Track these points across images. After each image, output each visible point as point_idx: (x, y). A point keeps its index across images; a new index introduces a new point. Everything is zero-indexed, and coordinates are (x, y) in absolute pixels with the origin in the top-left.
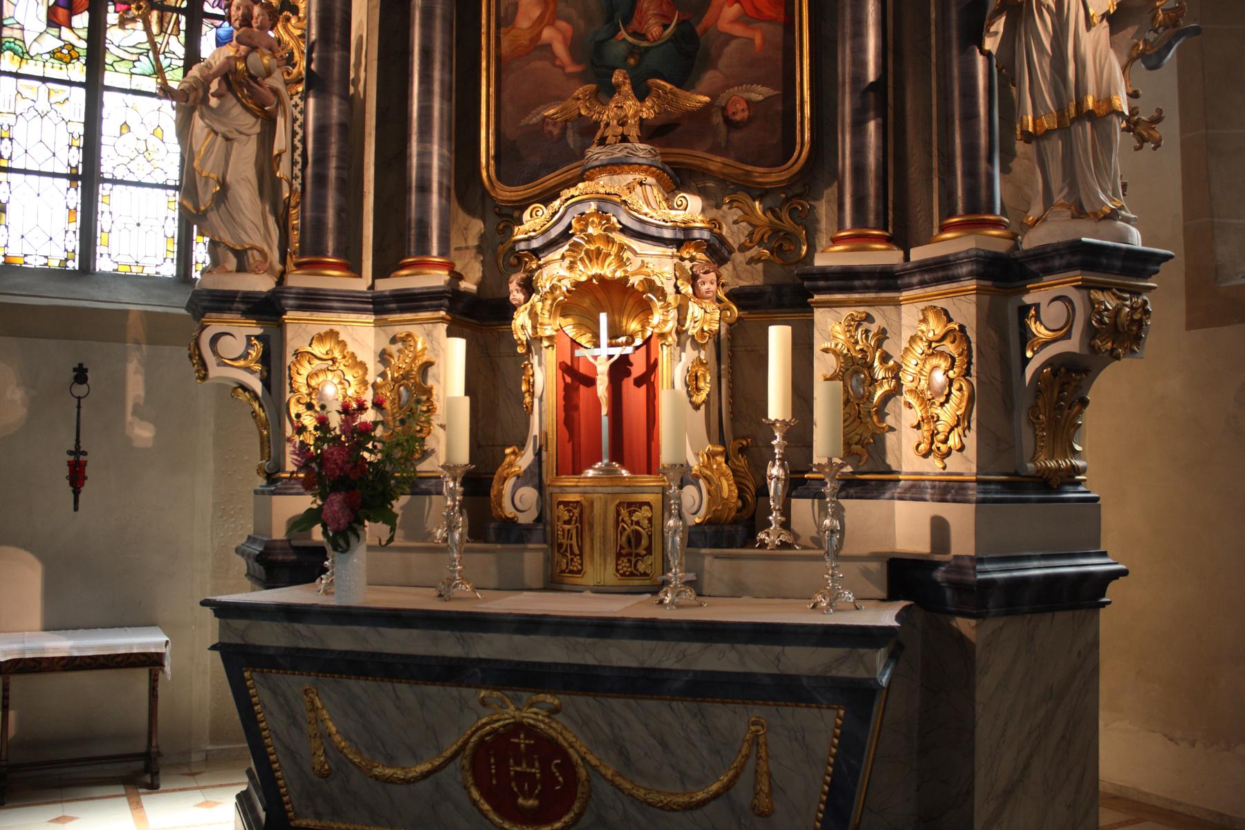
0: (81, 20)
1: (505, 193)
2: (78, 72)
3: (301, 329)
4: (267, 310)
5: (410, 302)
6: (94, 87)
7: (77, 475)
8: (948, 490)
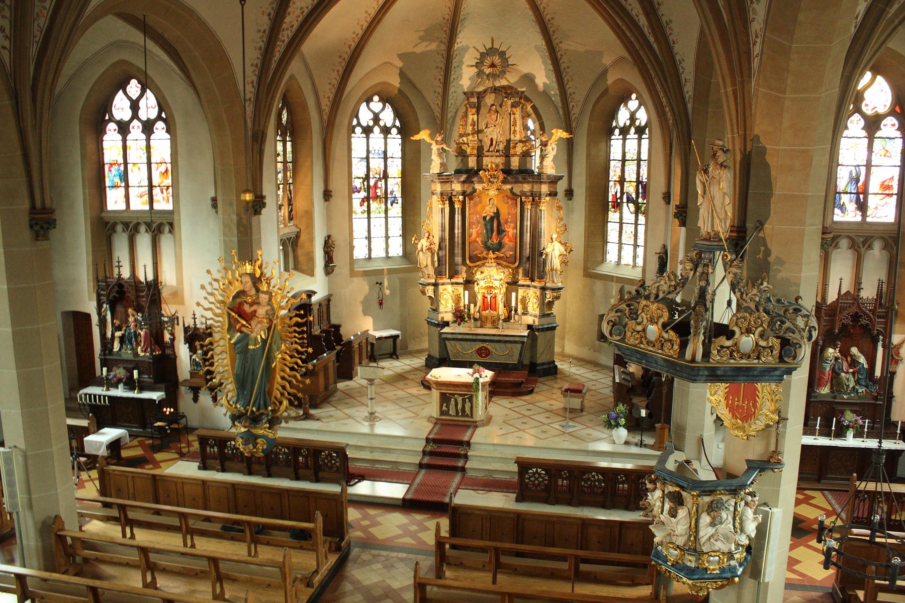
0: (366, 204)
1: (471, 265)
2: (366, 215)
3: (441, 288)
4: (436, 285)
5: (457, 284)
6: (369, 218)
7: (381, 304)
8: (535, 316)
